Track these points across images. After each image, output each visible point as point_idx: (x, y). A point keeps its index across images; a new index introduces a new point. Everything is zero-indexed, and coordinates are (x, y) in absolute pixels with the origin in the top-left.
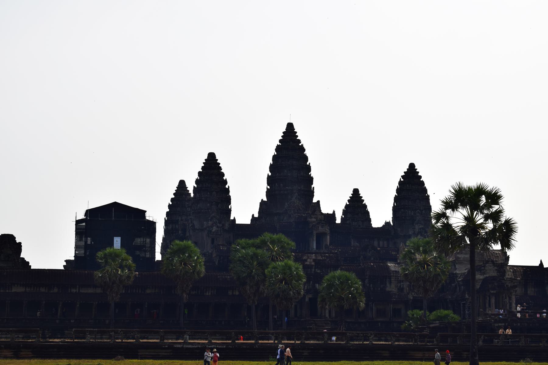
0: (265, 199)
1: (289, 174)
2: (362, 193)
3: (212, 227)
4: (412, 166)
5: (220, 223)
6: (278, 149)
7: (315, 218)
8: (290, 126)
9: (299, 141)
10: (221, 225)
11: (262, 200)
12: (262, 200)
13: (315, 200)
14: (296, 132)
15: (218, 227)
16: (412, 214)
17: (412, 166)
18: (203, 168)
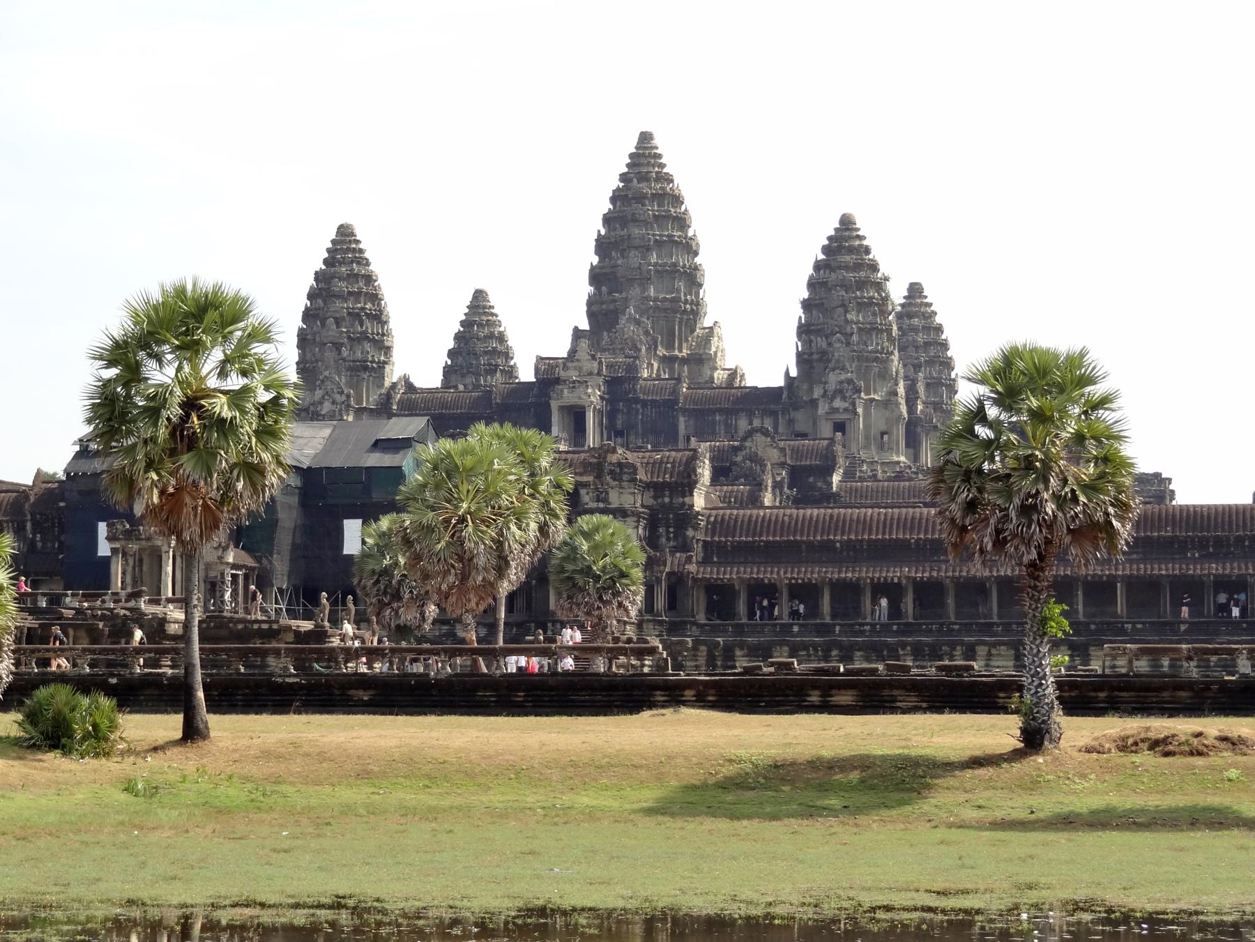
0: (584, 325)
1: (619, 262)
2: (932, 295)
3: (321, 403)
4: (847, 223)
5: (342, 393)
6: (616, 198)
7: (575, 368)
8: (645, 138)
9: (669, 179)
10: (344, 398)
11: (576, 330)
12: (576, 330)
13: (707, 322)
14: (660, 156)
15: (334, 403)
16: (824, 345)
17: (847, 223)
18: (325, 262)
